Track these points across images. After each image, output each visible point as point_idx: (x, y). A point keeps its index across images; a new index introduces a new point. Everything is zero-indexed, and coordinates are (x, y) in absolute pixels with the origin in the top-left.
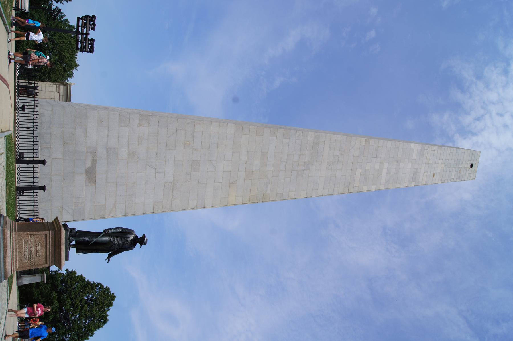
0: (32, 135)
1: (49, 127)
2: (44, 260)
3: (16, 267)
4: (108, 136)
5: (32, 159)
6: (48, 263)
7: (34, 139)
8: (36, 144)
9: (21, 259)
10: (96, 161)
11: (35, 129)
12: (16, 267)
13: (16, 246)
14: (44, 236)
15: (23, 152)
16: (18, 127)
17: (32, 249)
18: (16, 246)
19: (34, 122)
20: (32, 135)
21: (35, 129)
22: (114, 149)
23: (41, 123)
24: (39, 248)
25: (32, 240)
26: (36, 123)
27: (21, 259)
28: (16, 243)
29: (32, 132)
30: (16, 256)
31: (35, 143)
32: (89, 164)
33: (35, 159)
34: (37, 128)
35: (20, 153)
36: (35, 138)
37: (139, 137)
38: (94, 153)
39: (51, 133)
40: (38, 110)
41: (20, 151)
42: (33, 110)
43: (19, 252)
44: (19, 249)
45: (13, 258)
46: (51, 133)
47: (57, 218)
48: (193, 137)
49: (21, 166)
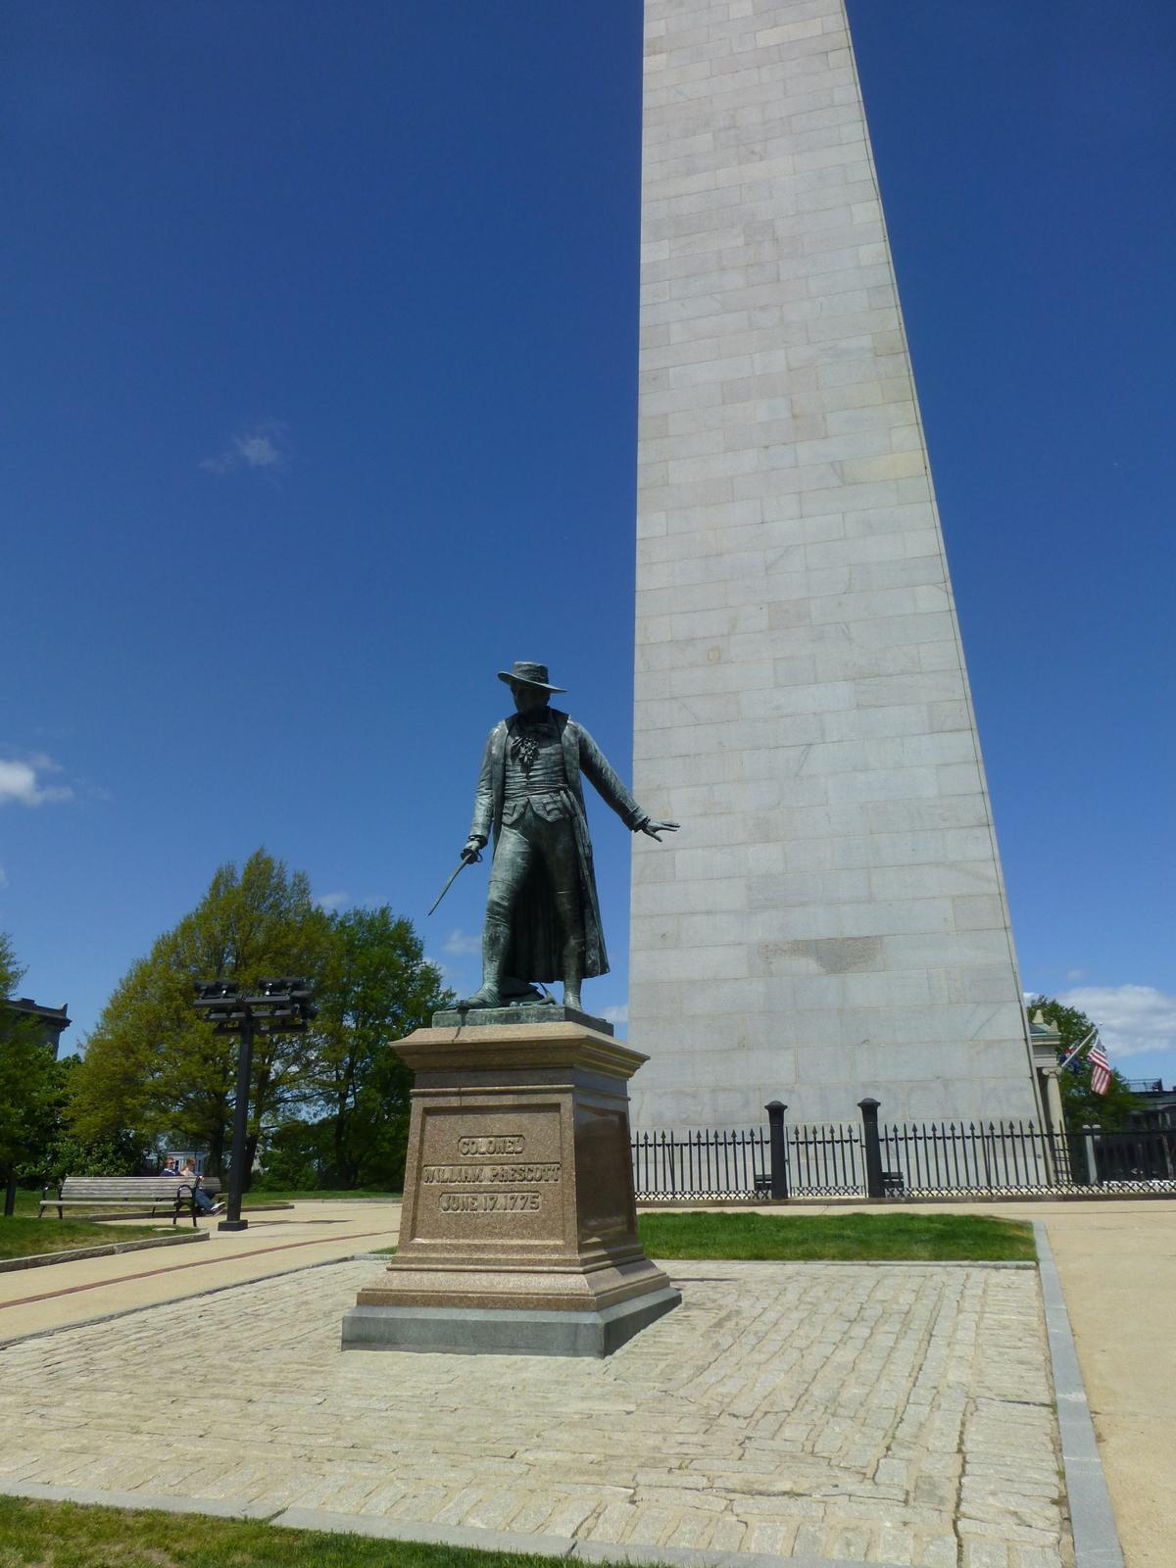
0: (686, 1149)
1: (694, 1096)
2: (542, 1118)
3: (556, 1249)
4: (708, 913)
5: (768, 1148)
6: (554, 1098)
7: (699, 1144)
8: (716, 1136)
9: (525, 1226)
10: (796, 942)
11: (668, 1140)
12: (556, 1249)
13: (457, 1248)
14: (430, 1120)
15: (756, 1179)
16: (674, 1193)
17: (487, 1171)
18: (457, 1248)
20: (686, 1149)
21: (668, 1140)
22: (750, 888)
27: (526, 1225)
28: (445, 1248)
29: (677, 1149)
30: (505, 1249)
32: (808, 965)
33: (767, 1136)
35: (758, 1187)
37: (704, 815)
38: (768, 952)
40: (827, 1130)
41: (751, 1186)
43: (492, 1235)
44: (475, 1232)
45: (507, 1262)
46: (714, 1091)
48: (691, 641)
49: (795, 1183)
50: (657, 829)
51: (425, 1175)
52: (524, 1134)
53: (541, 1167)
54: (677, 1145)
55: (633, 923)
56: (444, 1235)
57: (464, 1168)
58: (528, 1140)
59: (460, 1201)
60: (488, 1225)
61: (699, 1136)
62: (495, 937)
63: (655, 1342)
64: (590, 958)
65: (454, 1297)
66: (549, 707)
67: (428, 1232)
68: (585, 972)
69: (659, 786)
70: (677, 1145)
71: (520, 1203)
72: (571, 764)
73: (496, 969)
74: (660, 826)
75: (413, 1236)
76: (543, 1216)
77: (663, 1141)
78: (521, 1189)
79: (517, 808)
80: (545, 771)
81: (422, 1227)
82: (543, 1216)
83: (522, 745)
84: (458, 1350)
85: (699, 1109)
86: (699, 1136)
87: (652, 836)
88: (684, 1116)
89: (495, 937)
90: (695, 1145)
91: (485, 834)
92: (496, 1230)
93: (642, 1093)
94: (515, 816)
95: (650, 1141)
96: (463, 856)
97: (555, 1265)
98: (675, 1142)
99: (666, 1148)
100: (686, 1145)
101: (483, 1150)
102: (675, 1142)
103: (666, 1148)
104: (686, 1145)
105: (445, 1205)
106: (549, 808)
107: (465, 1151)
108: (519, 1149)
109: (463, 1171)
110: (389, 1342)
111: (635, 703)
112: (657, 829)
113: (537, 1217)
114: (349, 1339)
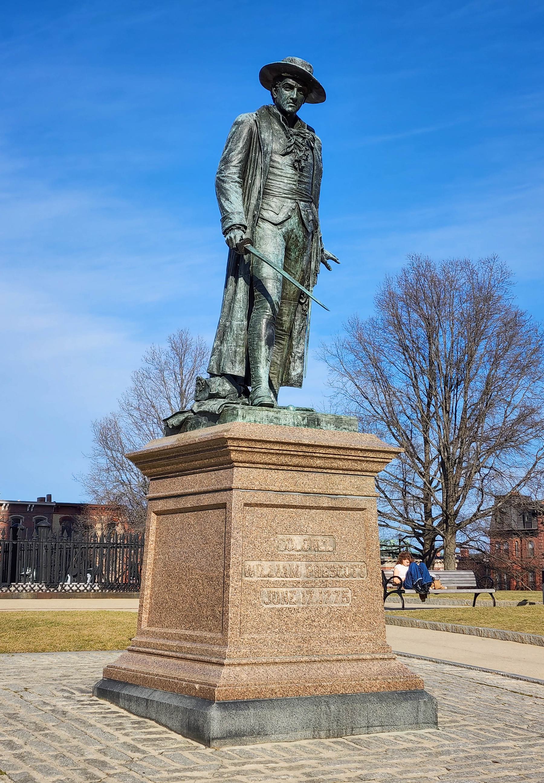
6: (362, 502)
24: (298, 541)
25: (266, 566)
27: (340, 619)
52: (334, 534)
57: (281, 564)
58: (337, 540)
67: (253, 627)
71: (333, 597)
92: (315, 624)
101: (299, 548)
108: (331, 549)
109: (281, 567)
114: (219, 736)
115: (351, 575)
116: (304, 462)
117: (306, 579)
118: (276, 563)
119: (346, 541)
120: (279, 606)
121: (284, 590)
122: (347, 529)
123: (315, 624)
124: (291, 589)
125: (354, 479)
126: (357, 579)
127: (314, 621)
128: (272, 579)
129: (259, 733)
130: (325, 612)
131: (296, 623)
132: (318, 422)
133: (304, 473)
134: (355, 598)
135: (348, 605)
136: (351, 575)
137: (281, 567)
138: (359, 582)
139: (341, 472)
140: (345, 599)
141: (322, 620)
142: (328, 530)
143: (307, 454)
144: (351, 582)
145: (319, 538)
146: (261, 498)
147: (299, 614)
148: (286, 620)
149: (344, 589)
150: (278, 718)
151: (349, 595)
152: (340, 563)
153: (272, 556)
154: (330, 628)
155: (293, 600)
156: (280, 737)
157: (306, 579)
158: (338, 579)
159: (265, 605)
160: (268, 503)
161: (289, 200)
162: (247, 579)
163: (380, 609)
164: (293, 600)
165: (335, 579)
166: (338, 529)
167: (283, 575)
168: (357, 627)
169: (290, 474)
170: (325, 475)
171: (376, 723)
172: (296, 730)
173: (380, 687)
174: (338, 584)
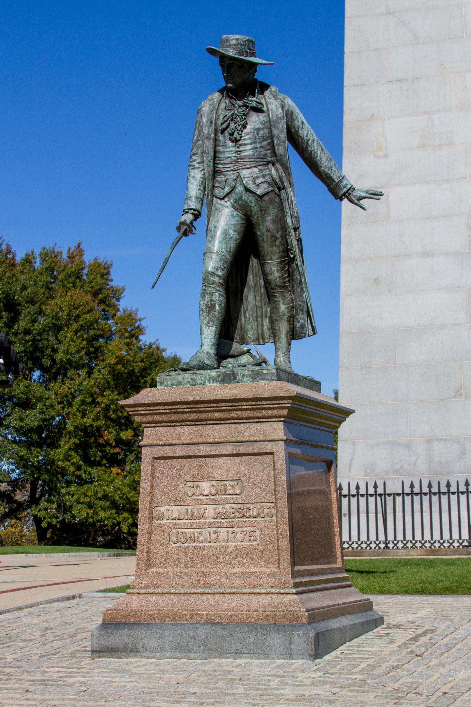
0: (399, 500)
1: (408, 447)
4: (426, 255)
6: (269, 447)
8: (430, 486)
17: (210, 510)
19: (449, 492)
20: (399, 500)
21: (380, 490)
23: (397, 472)
24: (206, 487)
25: (175, 511)
26: (358, 488)
27: (246, 555)
29: (389, 500)
31: (425, 490)
34: (376, 486)
36: (407, 490)
37: (422, 146)
39: (429, 441)
42: (353, 500)
46: (429, 441)
47: (352, 412)
50: (360, 198)
51: (155, 513)
52: (243, 479)
53: (258, 506)
54: (389, 495)
55: (344, 268)
56: (175, 564)
57: (190, 508)
59: (188, 536)
60: (213, 555)
61: (412, 486)
62: (211, 304)
63: (358, 650)
64: (299, 322)
65: (186, 615)
66: (256, 79)
67: (161, 562)
68: (294, 335)
69: (373, 116)
70: (389, 495)
71: (240, 536)
72: (279, 138)
73: (213, 334)
74: (364, 195)
75: (149, 566)
76: (261, 547)
77: (376, 492)
78: (241, 525)
79: (228, 182)
80: (254, 145)
81: (156, 558)
82: (261, 547)
83: (232, 120)
84: (190, 655)
85: (413, 459)
86: (412, 486)
87: (356, 204)
88: (398, 467)
89: (211, 304)
90: (408, 494)
91: (198, 207)
92: (220, 560)
93: (354, 444)
94: (227, 190)
95: (362, 491)
96: (178, 229)
97: (272, 587)
98: (387, 492)
99: (379, 498)
100: (398, 495)
101: (206, 492)
102: (387, 492)
103: (379, 498)
104: (398, 495)
105: (175, 539)
106: (259, 181)
107: (190, 494)
108: (238, 492)
109: (189, 511)
110: (132, 651)
111: (346, 20)
112: (360, 198)
113: (255, 549)
114: (98, 650)
115: (258, 516)
116: (203, 416)
117: (213, 520)
118: (185, 507)
119: (254, 484)
120: (186, 545)
121: (192, 530)
122: (255, 473)
123: (220, 560)
124: (199, 530)
125: (259, 426)
126: (266, 519)
127: (220, 558)
128: (181, 522)
129: (131, 650)
130: (230, 549)
131: (202, 559)
132: (233, 376)
133: (209, 426)
134: (262, 536)
135: (256, 543)
136: (258, 516)
137: (189, 511)
138: (266, 521)
139: (245, 421)
140: (252, 538)
141: (227, 557)
142: (235, 475)
143: (201, 409)
144: (259, 522)
145: (228, 483)
146: (168, 451)
147: (204, 552)
148: (192, 557)
149: (252, 529)
150: (148, 638)
151: (257, 534)
152: (248, 505)
153: (180, 502)
154: (234, 564)
155: (200, 540)
156: (151, 654)
157: (213, 520)
158: (245, 519)
159: (173, 545)
160: (174, 455)
161: (232, 172)
162: (157, 522)
163: (284, 547)
164: (200, 540)
165: (242, 520)
166: (246, 473)
167: (190, 517)
168: (263, 564)
169: (195, 428)
170: (230, 425)
171: (245, 650)
172: (165, 650)
173: (258, 618)
174: (244, 524)
